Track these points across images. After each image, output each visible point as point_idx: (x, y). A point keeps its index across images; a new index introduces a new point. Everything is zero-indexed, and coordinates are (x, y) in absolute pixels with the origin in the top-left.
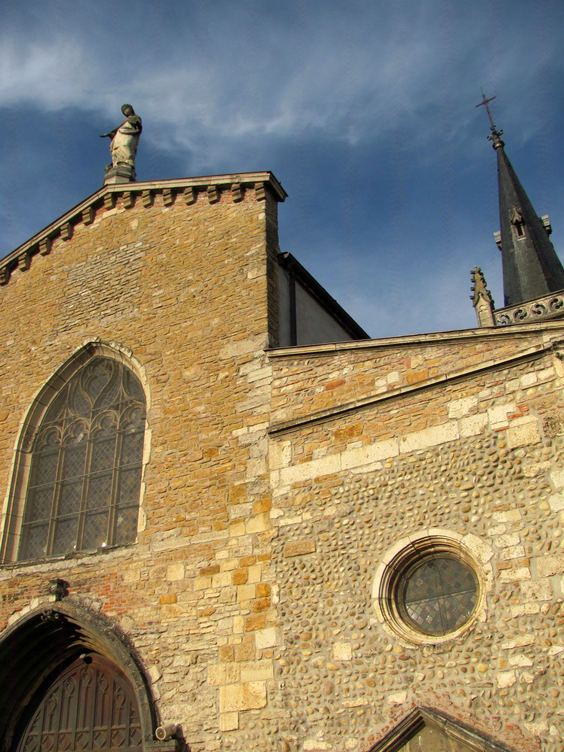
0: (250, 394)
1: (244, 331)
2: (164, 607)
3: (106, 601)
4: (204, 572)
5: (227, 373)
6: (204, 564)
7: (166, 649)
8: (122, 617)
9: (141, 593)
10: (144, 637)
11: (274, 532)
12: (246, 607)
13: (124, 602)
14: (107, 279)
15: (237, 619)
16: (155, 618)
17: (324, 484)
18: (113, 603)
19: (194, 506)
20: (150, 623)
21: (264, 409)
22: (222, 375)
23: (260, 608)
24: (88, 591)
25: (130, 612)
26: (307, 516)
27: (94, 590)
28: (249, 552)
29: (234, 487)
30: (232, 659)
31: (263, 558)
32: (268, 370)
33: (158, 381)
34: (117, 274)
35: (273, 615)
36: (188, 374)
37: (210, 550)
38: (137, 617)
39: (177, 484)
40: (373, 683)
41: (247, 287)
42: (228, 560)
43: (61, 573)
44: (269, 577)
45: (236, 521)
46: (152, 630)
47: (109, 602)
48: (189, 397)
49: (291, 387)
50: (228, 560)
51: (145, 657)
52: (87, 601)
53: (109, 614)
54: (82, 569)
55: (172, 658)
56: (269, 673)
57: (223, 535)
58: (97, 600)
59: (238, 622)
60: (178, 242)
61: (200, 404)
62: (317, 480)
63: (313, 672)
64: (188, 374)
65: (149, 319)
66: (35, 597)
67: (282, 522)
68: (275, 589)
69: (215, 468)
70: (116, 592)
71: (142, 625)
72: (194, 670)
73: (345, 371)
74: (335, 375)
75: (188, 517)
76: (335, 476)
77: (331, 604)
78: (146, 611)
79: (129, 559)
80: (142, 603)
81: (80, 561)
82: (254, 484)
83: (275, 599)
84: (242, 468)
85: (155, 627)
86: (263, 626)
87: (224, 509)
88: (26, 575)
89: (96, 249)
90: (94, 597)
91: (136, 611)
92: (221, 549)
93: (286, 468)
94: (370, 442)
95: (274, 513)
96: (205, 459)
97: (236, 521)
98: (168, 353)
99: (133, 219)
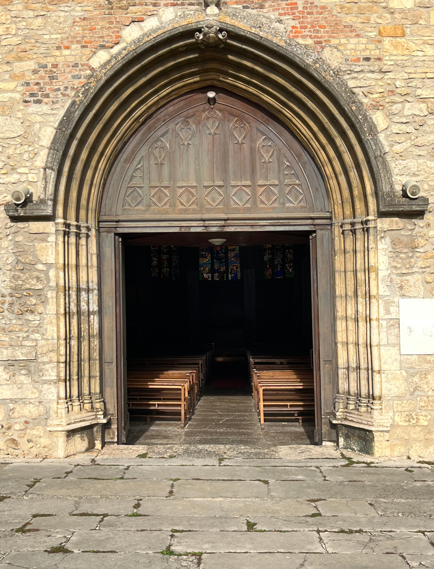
2: (387, 42)
3: (293, 23)
8: (323, 48)
9: (349, 19)
10: (362, 75)
13: (324, 27)
16: (376, 53)
18: (306, 27)
20: (367, 59)
24: (262, 7)
25: (334, 42)
27: (270, 6)
38: (346, 50)
46: (371, 68)
47: (298, 26)
51: (365, 101)
52: (264, 20)
53: (300, 41)
55: (400, 105)
58: (280, 21)
66: (166, 5)
70: (309, 13)
71: (355, 61)
78: (358, 43)
80: (352, 31)
85: (376, 66)
90: (273, 17)
91: (343, 41)
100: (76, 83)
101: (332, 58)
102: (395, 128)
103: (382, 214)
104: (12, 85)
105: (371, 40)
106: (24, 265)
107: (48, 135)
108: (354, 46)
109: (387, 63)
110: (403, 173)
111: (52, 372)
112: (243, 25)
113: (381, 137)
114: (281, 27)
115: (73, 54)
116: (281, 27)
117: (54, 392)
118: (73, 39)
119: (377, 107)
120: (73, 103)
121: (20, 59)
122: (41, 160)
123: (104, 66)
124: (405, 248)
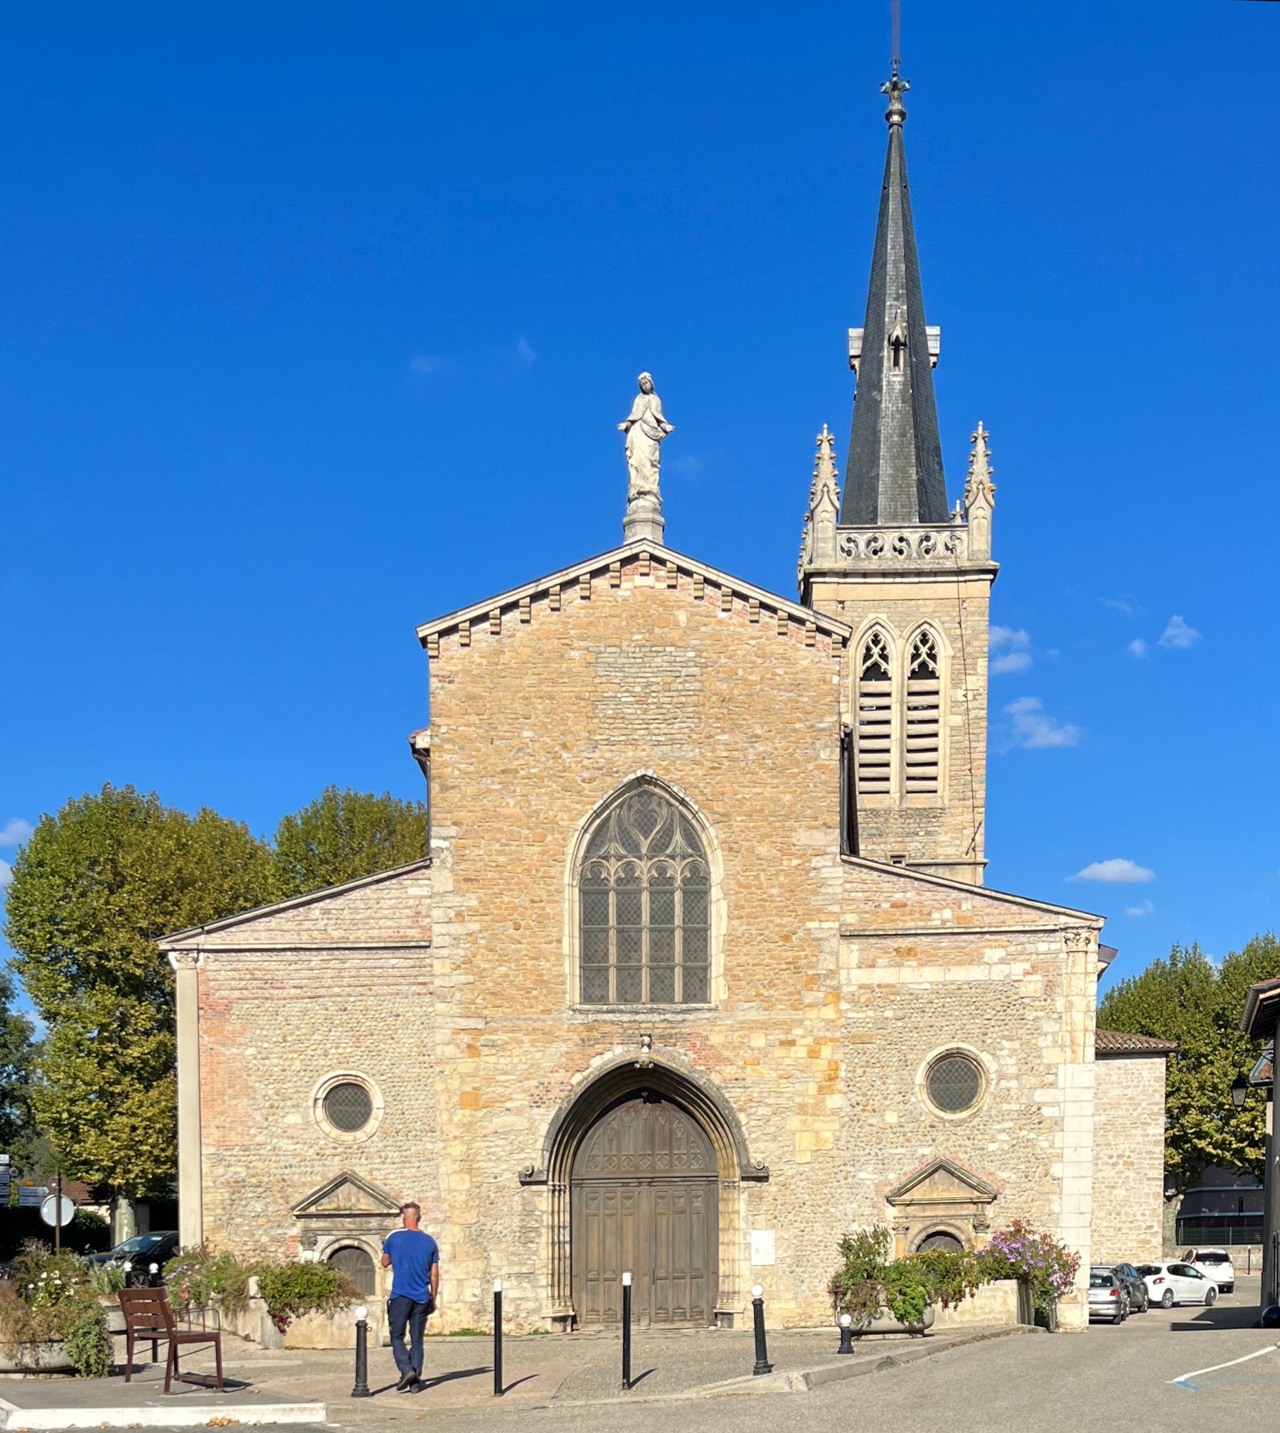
0: (822, 890)
1: (816, 819)
2: (749, 1068)
4: (782, 1043)
5: (800, 861)
6: (782, 1037)
7: (751, 1101)
9: (726, 1054)
11: (843, 1021)
12: (820, 1076)
14: (653, 688)
15: (811, 1085)
17: (884, 990)
19: (772, 985)
21: (836, 908)
22: (795, 862)
23: (831, 1079)
26: (871, 1013)
28: (821, 1034)
29: (807, 975)
30: (806, 1113)
31: (831, 1040)
32: (839, 871)
33: (731, 849)
34: (667, 687)
35: (841, 1086)
36: (762, 850)
37: (788, 1026)
39: (756, 961)
40: (908, 1141)
41: (818, 767)
42: (803, 1037)
43: (643, 1025)
44: (838, 1056)
45: (809, 1006)
48: (763, 876)
49: (860, 894)
50: (803, 1037)
54: (664, 1025)
56: (836, 1126)
57: (798, 1015)
59: (812, 1088)
60: (740, 672)
61: (773, 887)
62: (879, 986)
63: (867, 1129)
64: (762, 850)
65: (713, 768)
67: (850, 1015)
68: (843, 1066)
69: (790, 954)
72: (774, 1119)
73: (908, 895)
74: (899, 896)
75: (766, 994)
76: (893, 986)
77: (884, 1084)
79: (712, 1022)
81: (662, 1017)
82: (826, 976)
83: (843, 1074)
84: (814, 959)
86: (832, 1092)
87: (799, 993)
88: (605, 1021)
89: (632, 634)
92: (797, 1027)
93: (853, 968)
94: (921, 965)
95: (844, 1006)
96: (781, 943)
97: (809, 1006)
98: (739, 819)
99: (679, 608)
100: (563, 1095)
101: (716, 1079)
102: (752, 1123)
103: (743, 1179)
104: (522, 1096)
105: (739, 1067)
106: (528, 1212)
107: (544, 1128)
108: (730, 1071)
109: (749, 1082)
110: (758, 1154)
111: (544, 1281)
112: (663, 1060)
113: (744, 1129)
114: (686, 1059)
115: (558, 1076)
116: (686, 1059)
117: (544, 1293)
118: (560, 1066)
119: (741, 1110)
120: (560, 1109)
121: (528, 1079)
122: (540, 1145)
123: (579, 1084)
124: (756, 1199)
